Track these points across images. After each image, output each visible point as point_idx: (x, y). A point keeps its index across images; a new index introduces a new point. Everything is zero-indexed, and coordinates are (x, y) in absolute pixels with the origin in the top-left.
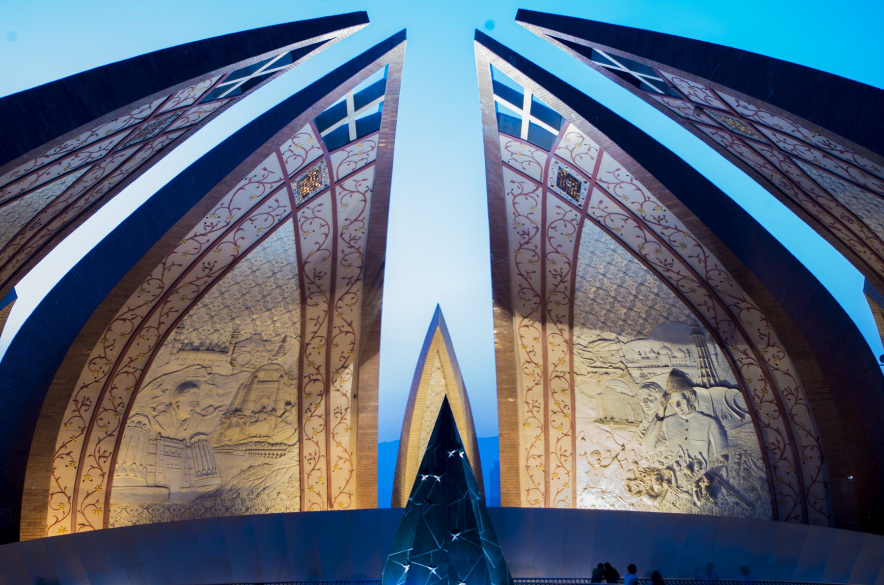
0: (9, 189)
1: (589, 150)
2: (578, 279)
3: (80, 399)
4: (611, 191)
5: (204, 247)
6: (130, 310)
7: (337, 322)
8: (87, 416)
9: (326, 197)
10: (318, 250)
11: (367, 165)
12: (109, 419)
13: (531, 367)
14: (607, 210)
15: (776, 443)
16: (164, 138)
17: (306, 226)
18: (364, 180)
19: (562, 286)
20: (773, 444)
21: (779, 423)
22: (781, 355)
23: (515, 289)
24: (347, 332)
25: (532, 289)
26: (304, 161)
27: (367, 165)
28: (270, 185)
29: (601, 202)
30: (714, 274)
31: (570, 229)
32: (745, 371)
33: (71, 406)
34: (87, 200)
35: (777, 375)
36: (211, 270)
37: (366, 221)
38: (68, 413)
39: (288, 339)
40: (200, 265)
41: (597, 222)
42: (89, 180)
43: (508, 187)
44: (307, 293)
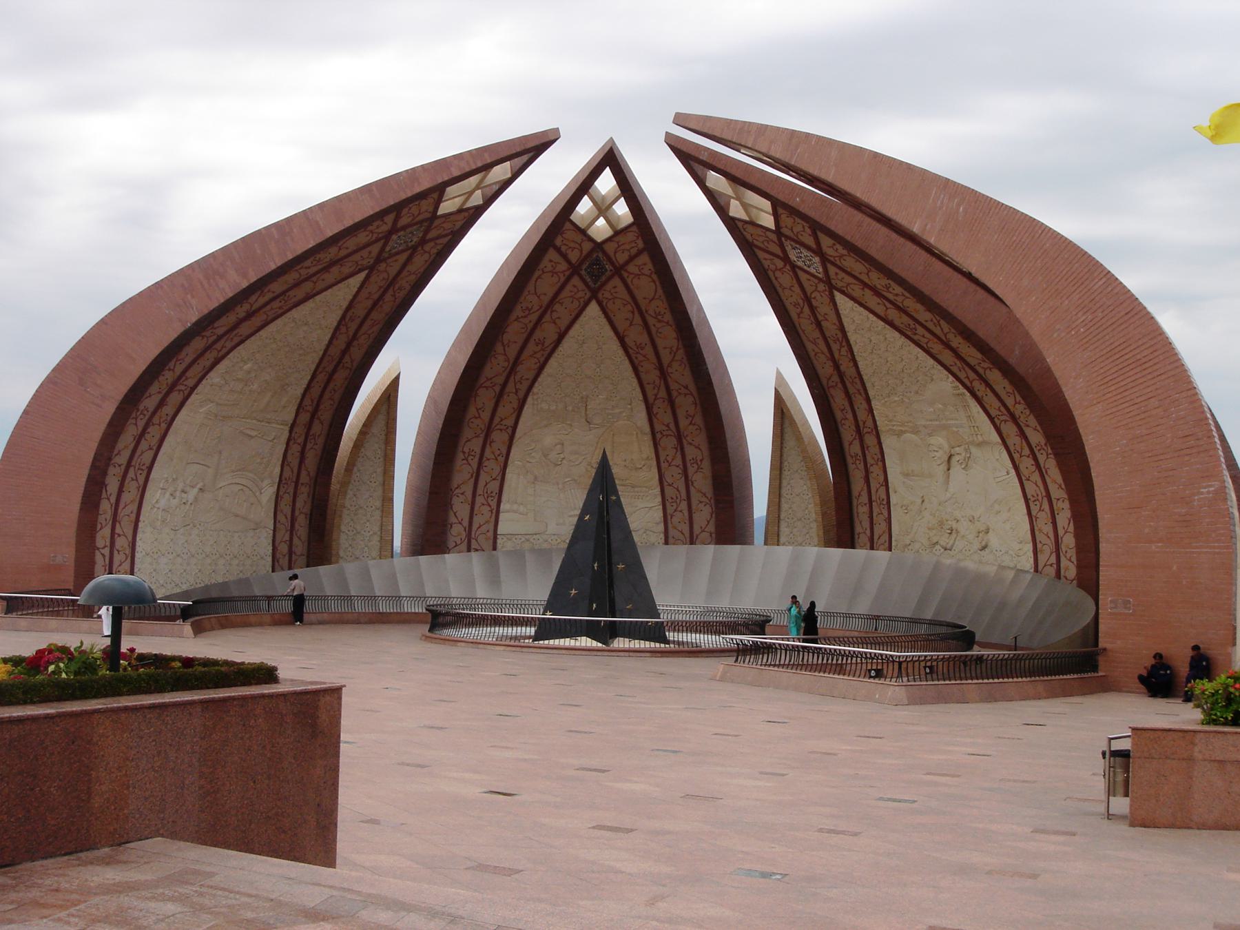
0: (291, 293)
3: (466, 450)
5: (530, 326)
6: (488, 379)
7: (673, 386)
8: (475, 466)
9: (616, 281)
11: (640, 253)
12: (492, 466)
16: (432, 244)
17: (610, 305)
21: (1036, 477)
22: (1028, 412)
23: (812, 354)
27: (640, 253)
30: (950, 336)
31: (826, 300)
32: (1003, 427)
33: (460, 456)
34: (394, 296)
35: (1028, 431)
37: (663, 297)
38: (459, 462)
40: (532, 341)
41: (843, 292)
42: (378, 281)
43: (766, 264)
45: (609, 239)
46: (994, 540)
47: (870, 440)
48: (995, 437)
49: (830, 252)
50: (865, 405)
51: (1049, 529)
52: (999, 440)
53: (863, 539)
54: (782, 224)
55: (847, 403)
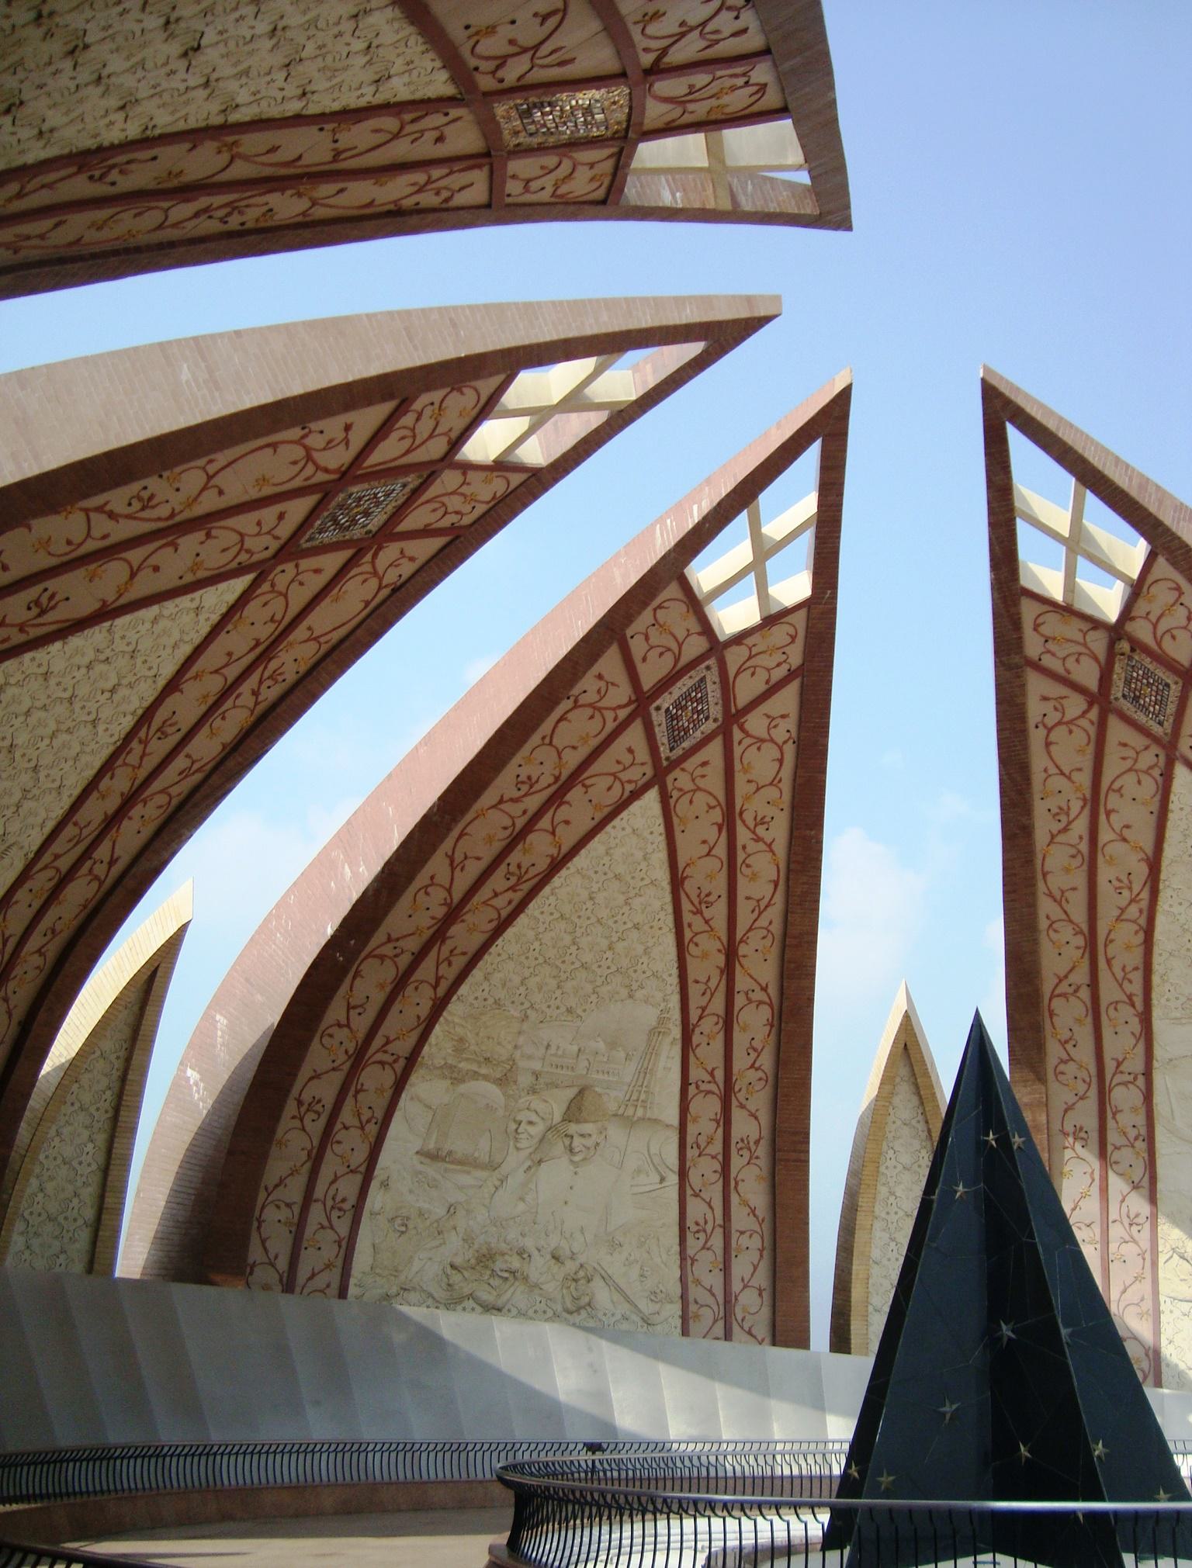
1: (778, 665)
2: (547, 890)
4: (737, 750)
5: (91, 546)
10: (216, 672)
13: (342, 1034)
14: (701, 783)
15: (702, 1222)
17: (252, 609)
18: (412, 559)
19: (510, 895)
20: (697, 1224)
21: (715, 1194)
22: (759, 1086)
24: (97, 878)
25: (449, 891)
26: (408, 452)
28: (310, 469)
29: (704, 764)
35: (737, 1114)
36: (43, 612)
37: (325, 648)
39: (14, 848)
40: (33, 592)
43: (588, 684)
44: (119, 762)
45: (468, 467)
46: (602, 1295)
47: (375, 1079)
48: (671, 1114)
49: (755, 723)
50: (424, 1010)
51: (716, 1280)
52: (675, 1122)
53: (263, 1274)
54: (749, 641)
55: (378, 998)
